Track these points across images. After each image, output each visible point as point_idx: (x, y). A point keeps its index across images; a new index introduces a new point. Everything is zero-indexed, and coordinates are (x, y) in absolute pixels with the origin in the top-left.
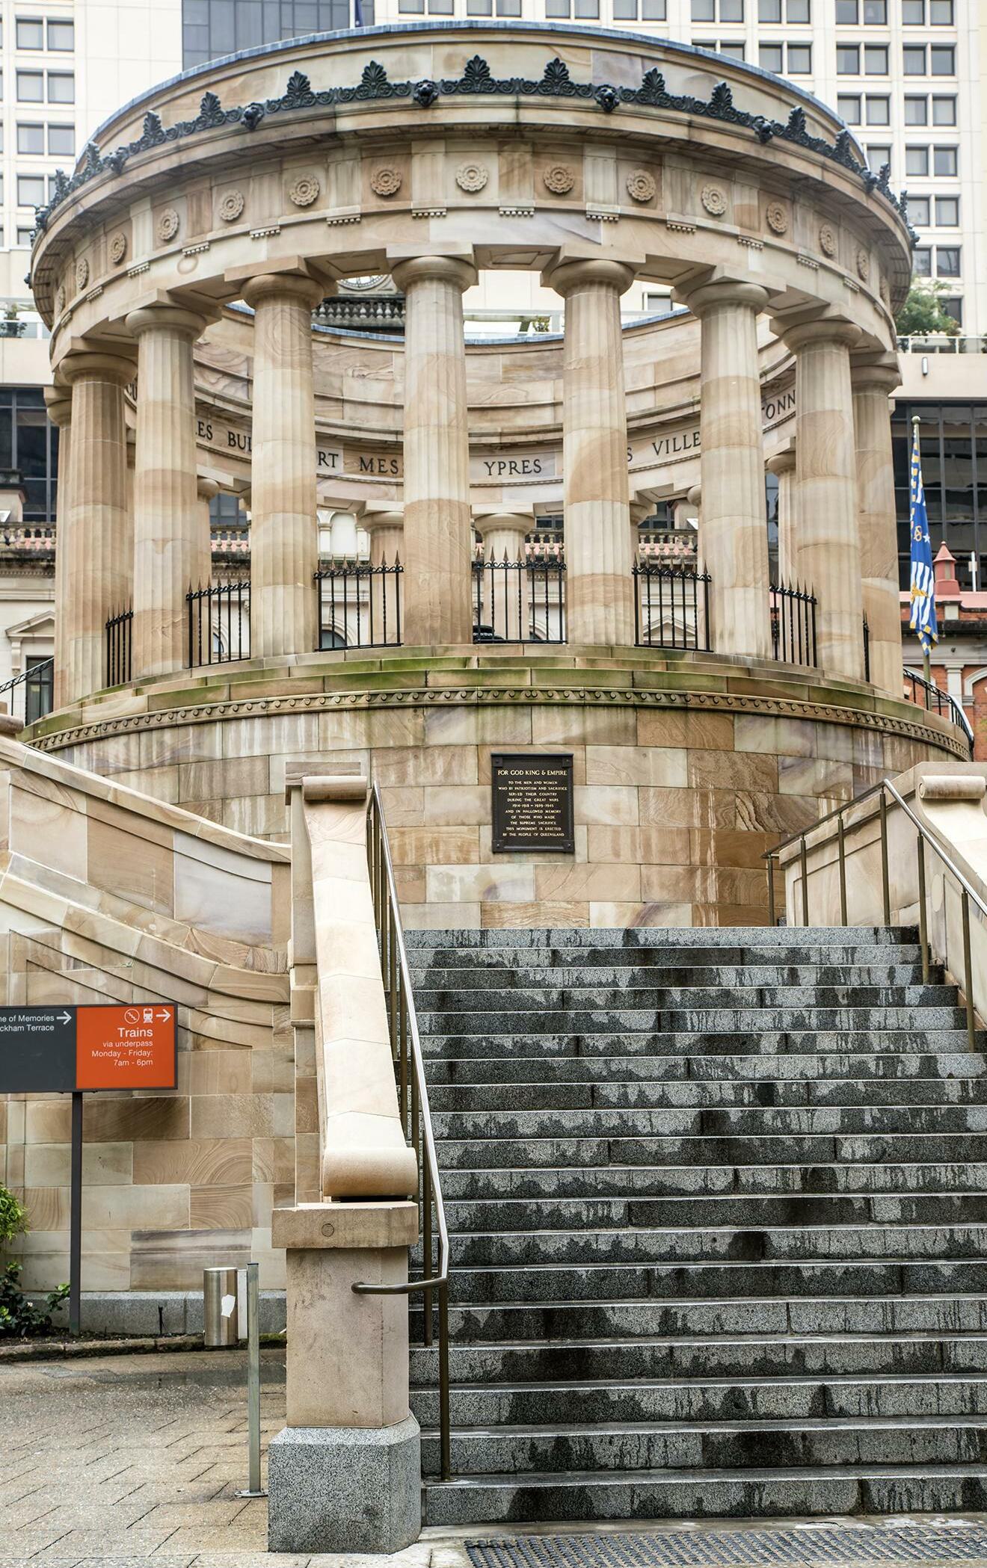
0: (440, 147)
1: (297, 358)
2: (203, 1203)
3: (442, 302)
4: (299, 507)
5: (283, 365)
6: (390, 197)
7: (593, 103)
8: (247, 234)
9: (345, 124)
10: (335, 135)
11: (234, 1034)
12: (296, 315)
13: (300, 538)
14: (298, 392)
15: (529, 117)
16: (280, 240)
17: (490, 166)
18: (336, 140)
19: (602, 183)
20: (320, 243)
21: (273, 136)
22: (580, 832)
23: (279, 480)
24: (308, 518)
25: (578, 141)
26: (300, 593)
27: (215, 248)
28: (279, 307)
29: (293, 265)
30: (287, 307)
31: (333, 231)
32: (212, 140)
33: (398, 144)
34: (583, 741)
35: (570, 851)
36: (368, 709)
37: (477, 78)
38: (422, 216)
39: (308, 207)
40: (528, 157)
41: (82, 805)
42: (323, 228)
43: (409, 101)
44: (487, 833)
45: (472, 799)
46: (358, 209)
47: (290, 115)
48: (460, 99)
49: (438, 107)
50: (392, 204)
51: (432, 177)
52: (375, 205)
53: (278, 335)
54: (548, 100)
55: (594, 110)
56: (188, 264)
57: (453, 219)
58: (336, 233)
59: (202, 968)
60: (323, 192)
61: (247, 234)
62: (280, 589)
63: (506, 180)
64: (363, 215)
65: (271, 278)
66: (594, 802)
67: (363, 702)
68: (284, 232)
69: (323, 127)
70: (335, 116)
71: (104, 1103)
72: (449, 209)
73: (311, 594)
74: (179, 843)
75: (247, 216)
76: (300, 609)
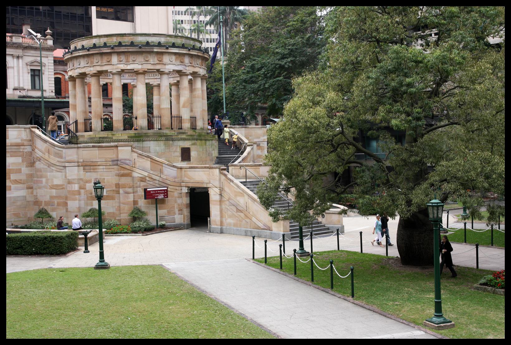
2: (169, 212)
9: (155, 50)
11: (172, 190)
17: (174, 57)
18: (153, 52)
19: (187, 60)
25: (184, 55)
33: (162, 53)
37: (174, 45)
38: (165, 65)
41: (149, 159)
44: (180, 159)
45: (178, 153)
50: (161, 62)
51: (166, 59)
57: (170, 66)
59: (168, 182)
63: (176, 60)
66: (193, 154)
69: (152, 50)
74: (164, 165)
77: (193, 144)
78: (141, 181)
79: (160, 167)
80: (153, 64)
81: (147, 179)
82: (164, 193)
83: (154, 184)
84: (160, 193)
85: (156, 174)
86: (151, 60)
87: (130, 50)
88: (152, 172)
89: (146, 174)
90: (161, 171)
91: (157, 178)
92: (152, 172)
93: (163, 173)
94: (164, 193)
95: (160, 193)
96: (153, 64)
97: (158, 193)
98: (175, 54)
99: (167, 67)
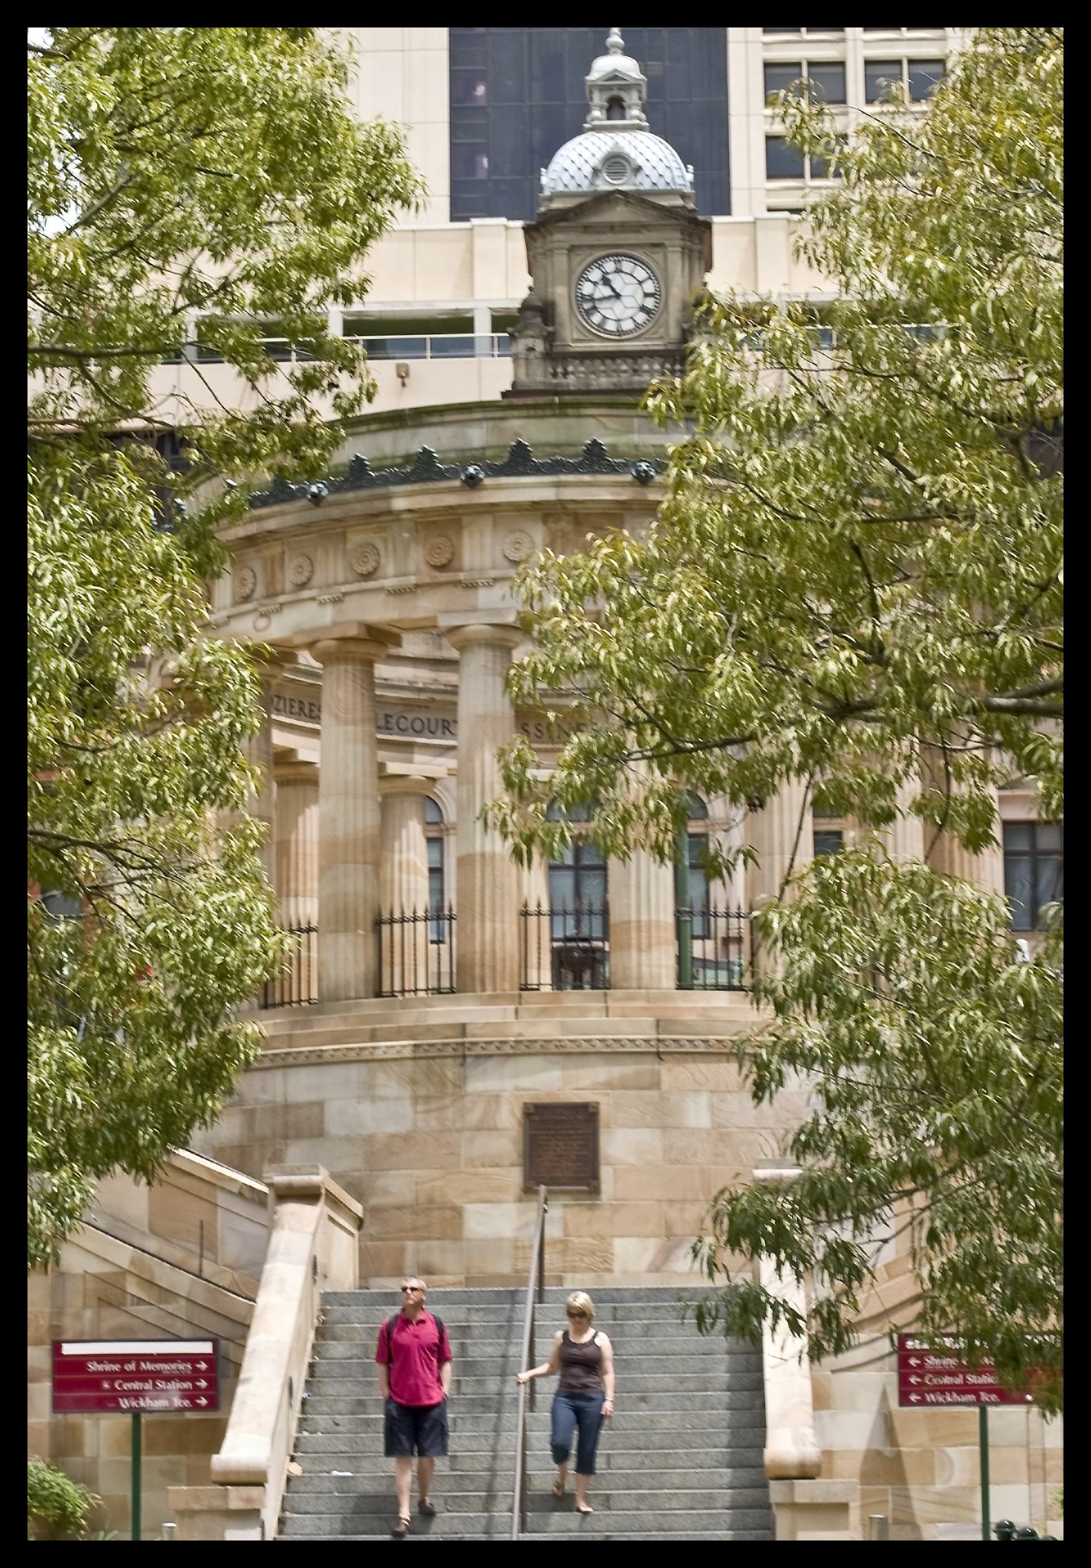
0: (487, 521)
1: (359, 715)
3: (490, 665)
4: (360, 857)
5: (346, 723)
6: (442, 568)
7: (629, 478)
8: (313, 599)
9: (399, 504)
10: (390, 512)
12: (359, 674)
13: (361, 888)
14: (359, 747)
15: (568, 494)
16: (344, 606)
20: (379, 611)
21: (336, 512)
22: (606, 1173)
23: (340, 833)
24: (369, 867)
26: (360, 941)
27: (286, 611)
28: (342, 668)
29: (353, 632)
30: (350, 668)
31: (391, 599)
32: (282, 514)
34: (609, 1085)
35: (595, 1191)
36: (414, 1059)
37: (519, 461)
38: (471, 586)
39: (368, 576)
40: (570, 528)
42: (382, 597)
43: (457, 483)
46: (413, 580)
47: (350, 495)
48: (504, 480)
49: (485, 488)
52: (427, 576)
53: (341, 695)
54: (587, 478)
55: (630, 484)
56: (262, 623)
58: (393, 601)
60: (383, 561)
61: (313, 599)
62: (342, 938)
64: (417, 586)
65: (333, 643)
66: (619, 1145)
67: (407, 1053)
68: (347, 599)
69: (379, 505)
70: (388, 497)
71: (164, 1422)
72: (495, 580)
73: (371, 940)
74: (221, 1198)
75: (316, 580)
76: (361, 955)
77: (623, 1084)
78: (103, 1302)
79: (197, 1211)
80: (398, 592)
81: (132, 1287)
82: (194, 1376)
83: (166, 1323)
84: (156, 1376)
85: (176, 1254)
86: (390, 568)
87: (271, 525)
88: (152, 1245)
89: (123, 1256)
90: (206, 1241)
91: (181, 1282)
92: (152, 1245)
93: (214, 1250)
94: (194, 1376)
95: (156, 1376)
96: (398, 592)
97: (142, 1376)
98: (544, 511)
99: (485, 597)
